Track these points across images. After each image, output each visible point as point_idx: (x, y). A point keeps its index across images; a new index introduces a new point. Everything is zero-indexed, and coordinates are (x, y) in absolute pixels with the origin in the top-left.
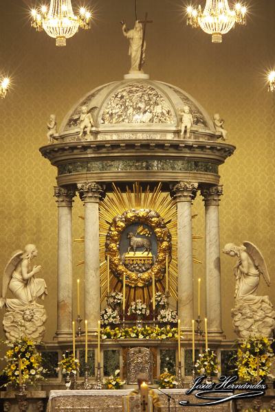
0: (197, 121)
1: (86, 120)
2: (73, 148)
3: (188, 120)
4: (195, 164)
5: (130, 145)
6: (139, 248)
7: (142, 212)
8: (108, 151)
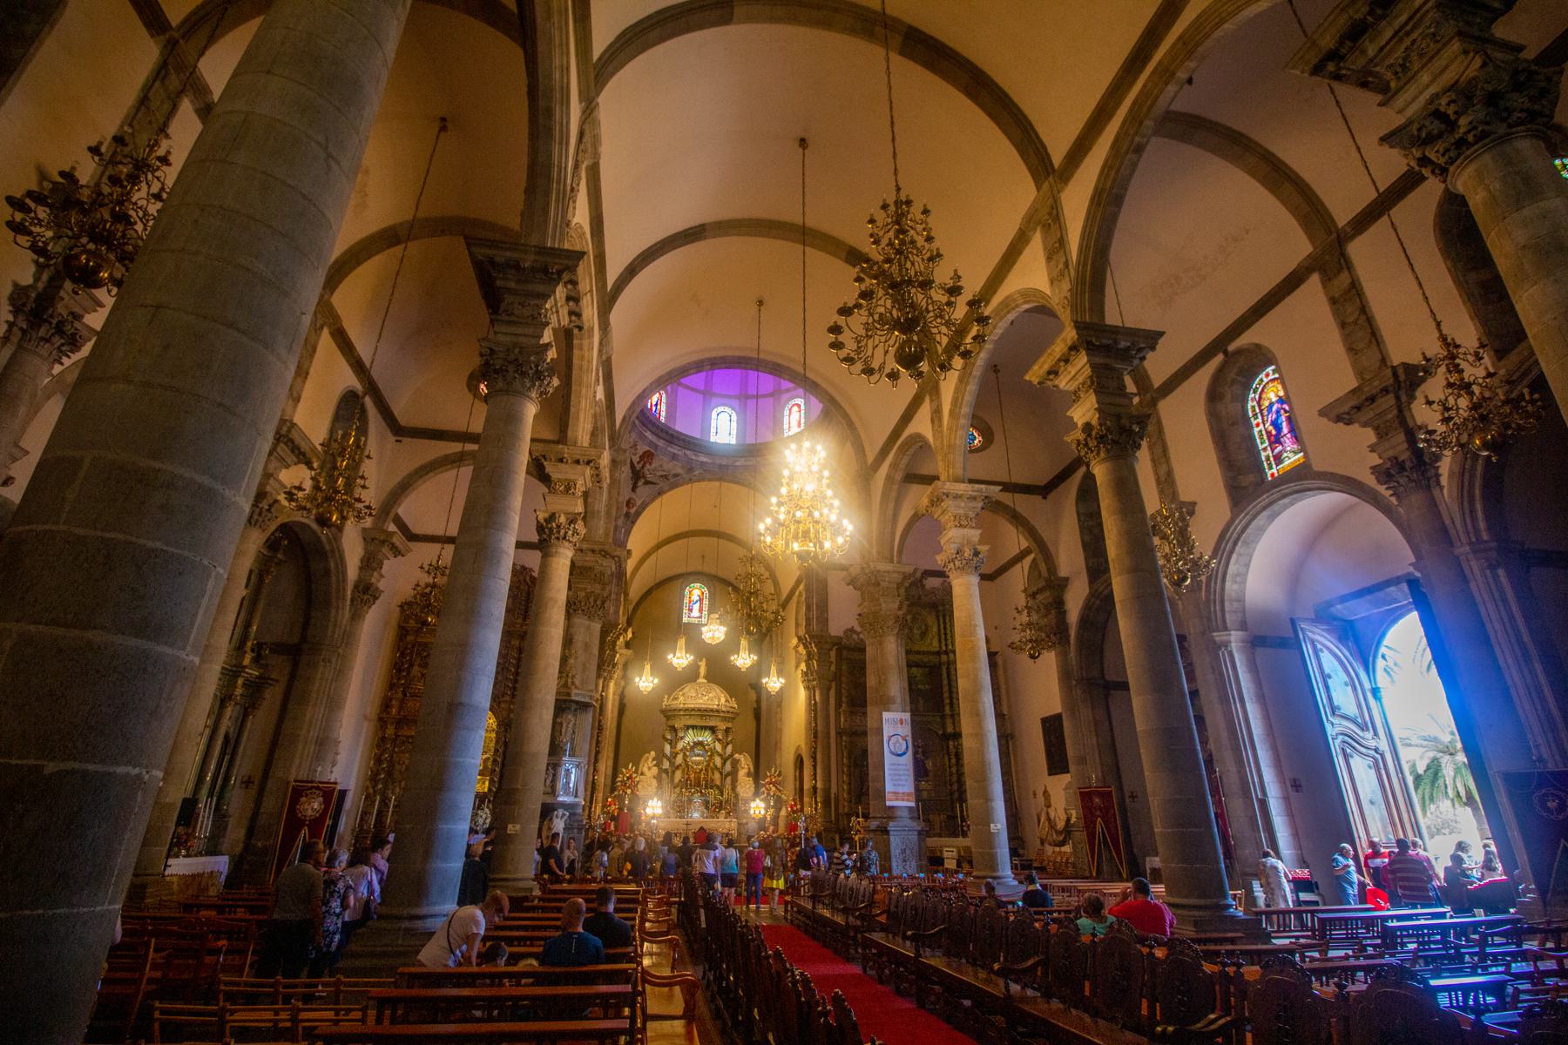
0: (727, 701)
1: (681, 698)
2: (675, 710)
3: (723, 700)
4: (725, 719)
5: (699, 710)
6: (698, 755)
7: (700, 739)
8: (689, 712)
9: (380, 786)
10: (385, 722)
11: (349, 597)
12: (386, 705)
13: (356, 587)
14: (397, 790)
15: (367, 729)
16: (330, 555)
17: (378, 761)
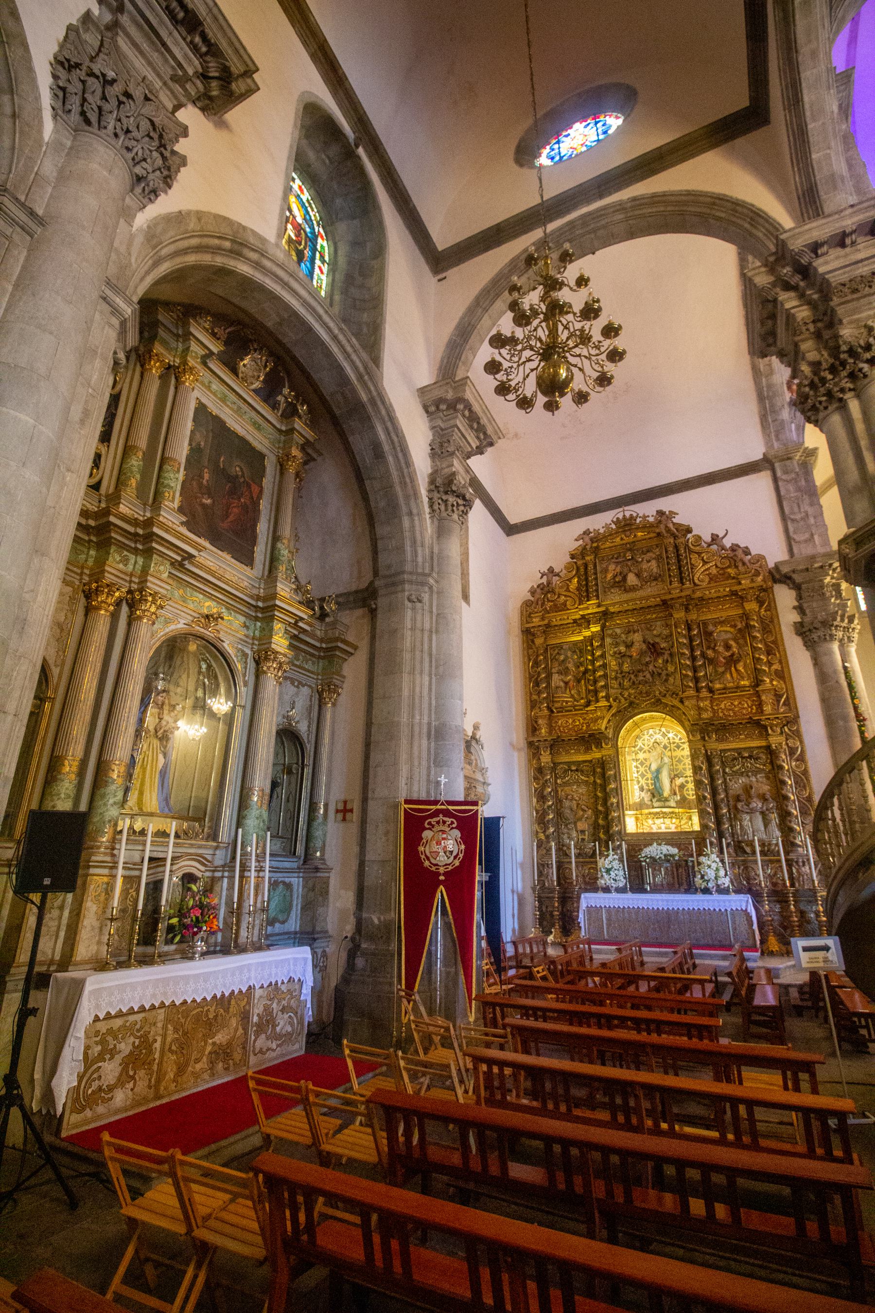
9: (552, 830)
10: (538, 748)
11: (425, 500)
12: (532, 728)
13: (432, 481)
14: (574, 834)
15: (519, 760)
16: (370, 409)
17: (542, 797)
